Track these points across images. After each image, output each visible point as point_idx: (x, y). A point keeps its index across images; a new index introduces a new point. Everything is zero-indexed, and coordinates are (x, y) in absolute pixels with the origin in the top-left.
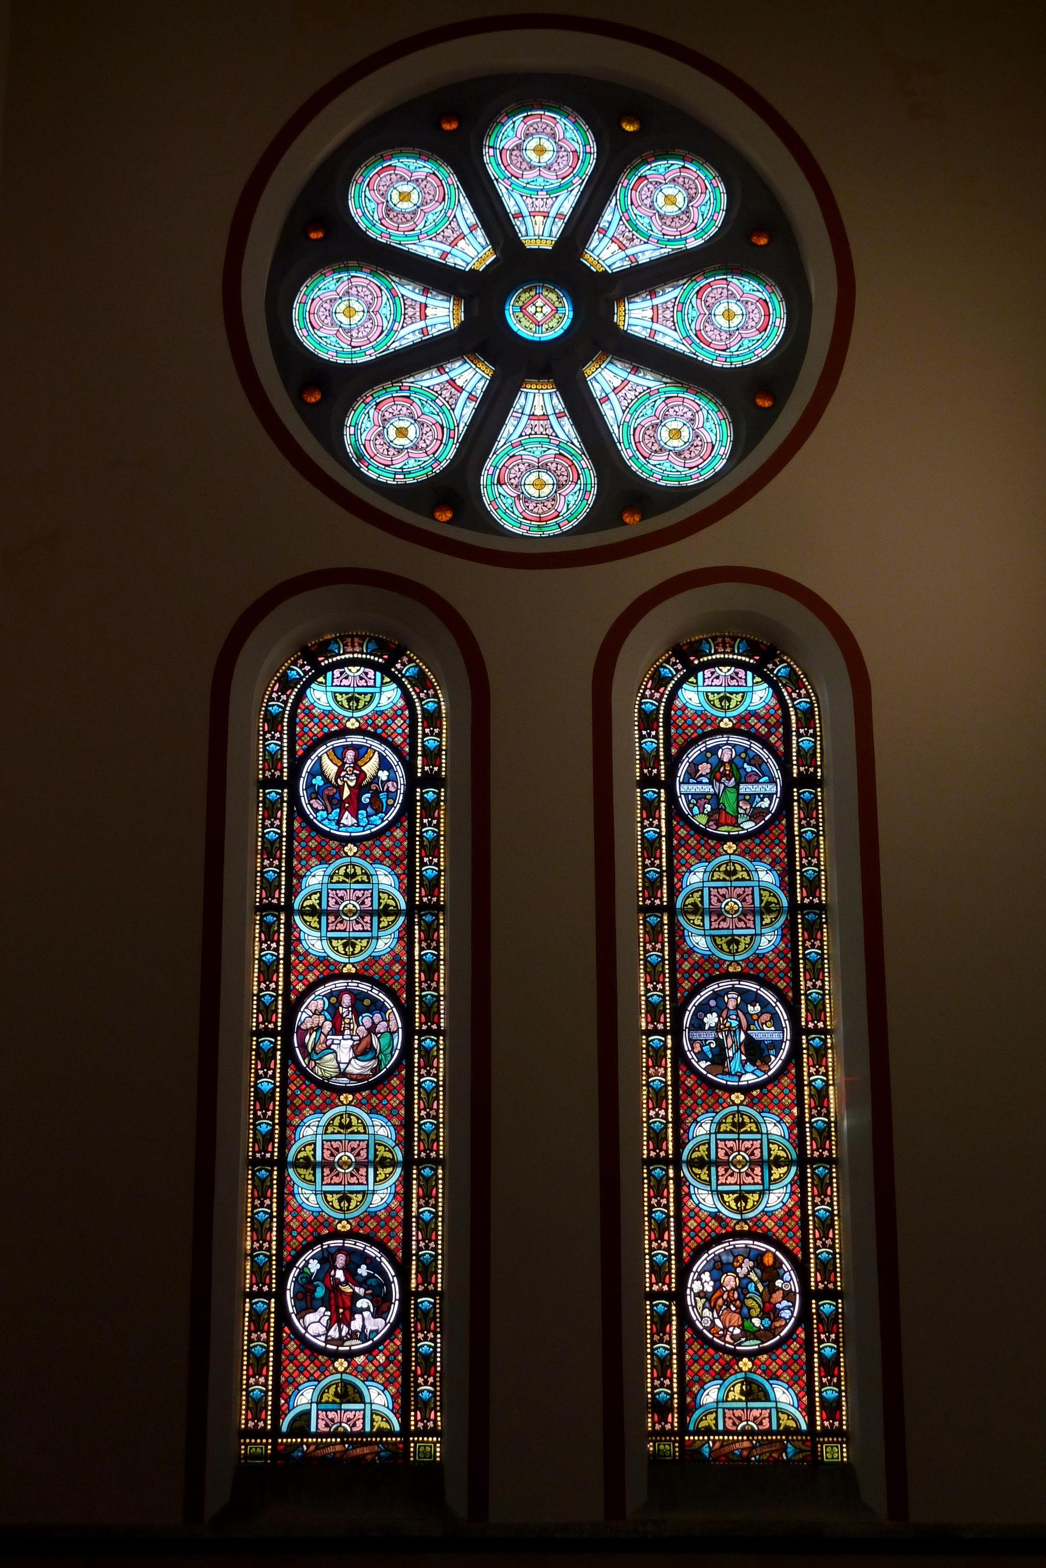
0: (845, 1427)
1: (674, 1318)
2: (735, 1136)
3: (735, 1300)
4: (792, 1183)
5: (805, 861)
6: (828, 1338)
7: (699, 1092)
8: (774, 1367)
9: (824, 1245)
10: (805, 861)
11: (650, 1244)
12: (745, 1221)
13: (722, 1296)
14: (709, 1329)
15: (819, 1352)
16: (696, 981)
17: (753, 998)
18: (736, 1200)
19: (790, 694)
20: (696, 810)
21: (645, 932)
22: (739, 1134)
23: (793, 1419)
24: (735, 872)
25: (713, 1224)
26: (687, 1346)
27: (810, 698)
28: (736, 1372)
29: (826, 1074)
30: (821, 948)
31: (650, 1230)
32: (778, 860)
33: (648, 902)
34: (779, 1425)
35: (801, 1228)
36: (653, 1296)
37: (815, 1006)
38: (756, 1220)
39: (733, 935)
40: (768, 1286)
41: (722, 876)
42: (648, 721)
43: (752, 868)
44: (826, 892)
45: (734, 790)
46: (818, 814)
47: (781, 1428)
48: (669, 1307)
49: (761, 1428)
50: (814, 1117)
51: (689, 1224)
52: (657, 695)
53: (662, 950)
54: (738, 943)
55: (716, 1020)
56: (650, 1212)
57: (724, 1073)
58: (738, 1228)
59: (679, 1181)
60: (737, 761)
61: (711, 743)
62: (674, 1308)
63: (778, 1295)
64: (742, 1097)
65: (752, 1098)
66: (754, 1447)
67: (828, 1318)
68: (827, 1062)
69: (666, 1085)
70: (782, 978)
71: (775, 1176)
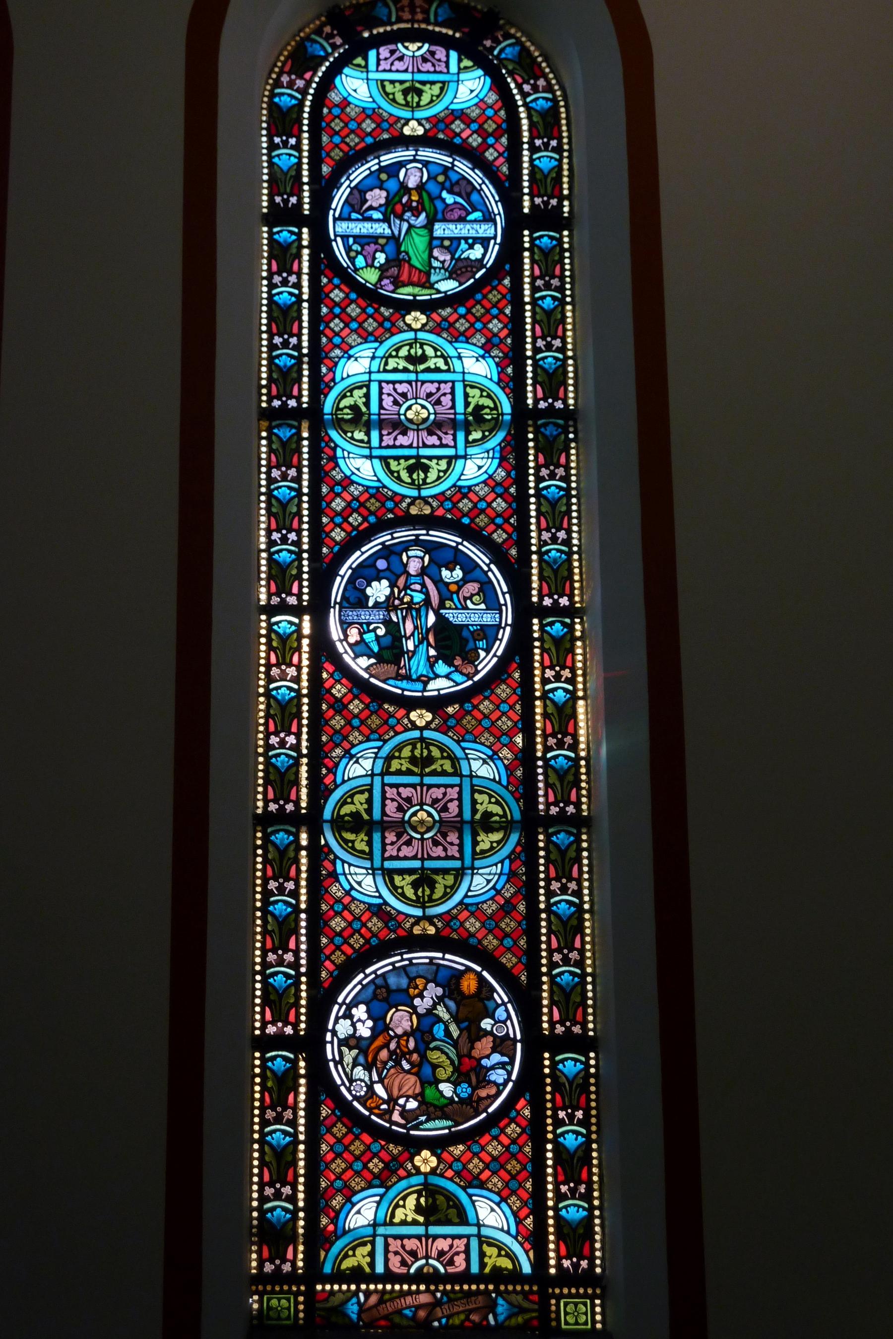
0: (598, 1270)
1: (303, 1081)
2: (416, 780)
3: (411, 1053)
4: (512, 857)
5: (540, 343)
6: (571, 1117)
7: (355, 706)
8: (475, 1165)
9: (566, 961)
10: (540, 343)
11: (264, 956)
12: (430, 919)
13: (386, 1045)
14: (362, 1100)
15: (555, 1142)
16: (355, 528)
17: (450, 555)
18: (415, 885)
19: (519, 87)
20: (360, 261)
21: (270, 451)
22: (422, 775)
23: (507, 1255)
24: (424, 358)
25: (375, 924)
26: (323, 1130)
27: (553, 92)
28: (409, 1175)
29: (572, 681)
30: (566, 479)
31: (264, 933)
32: (496, 340)
33: (276, 403)
34: (482, 1265)
35: (526, 932)
36: (266, 1043)
37: (556, 572)
38: (447, 917)
39: (418, 457)
40: (468, 1029)
41: (402, 364)
42: (283, 123)
43: (452, 352)
44: (576, 391)
45: (424, 232)
46: (563, 270)
47: (487, 1270)
48: (295, 1062)
49: (451, 1270)
50: (551, 749)
51: (333, 924)
52: (300, 83)
53: (298, 479)
54: (426, 469)
55: (387, 591)
56: (266, 902)
57: (398, 677)
58: (417, 930)
59: (318, 852)
60: (432, 187)
61: (388, 159)
62: (302, 1064)
63: (486, 1044)
64: (429, 716)
65: (447, 717)
66: (438, 1303)
67: (571, 1083)
68: (574, 661)
69: (299, 695)
70: (499, 527)
71: (484, 846)
